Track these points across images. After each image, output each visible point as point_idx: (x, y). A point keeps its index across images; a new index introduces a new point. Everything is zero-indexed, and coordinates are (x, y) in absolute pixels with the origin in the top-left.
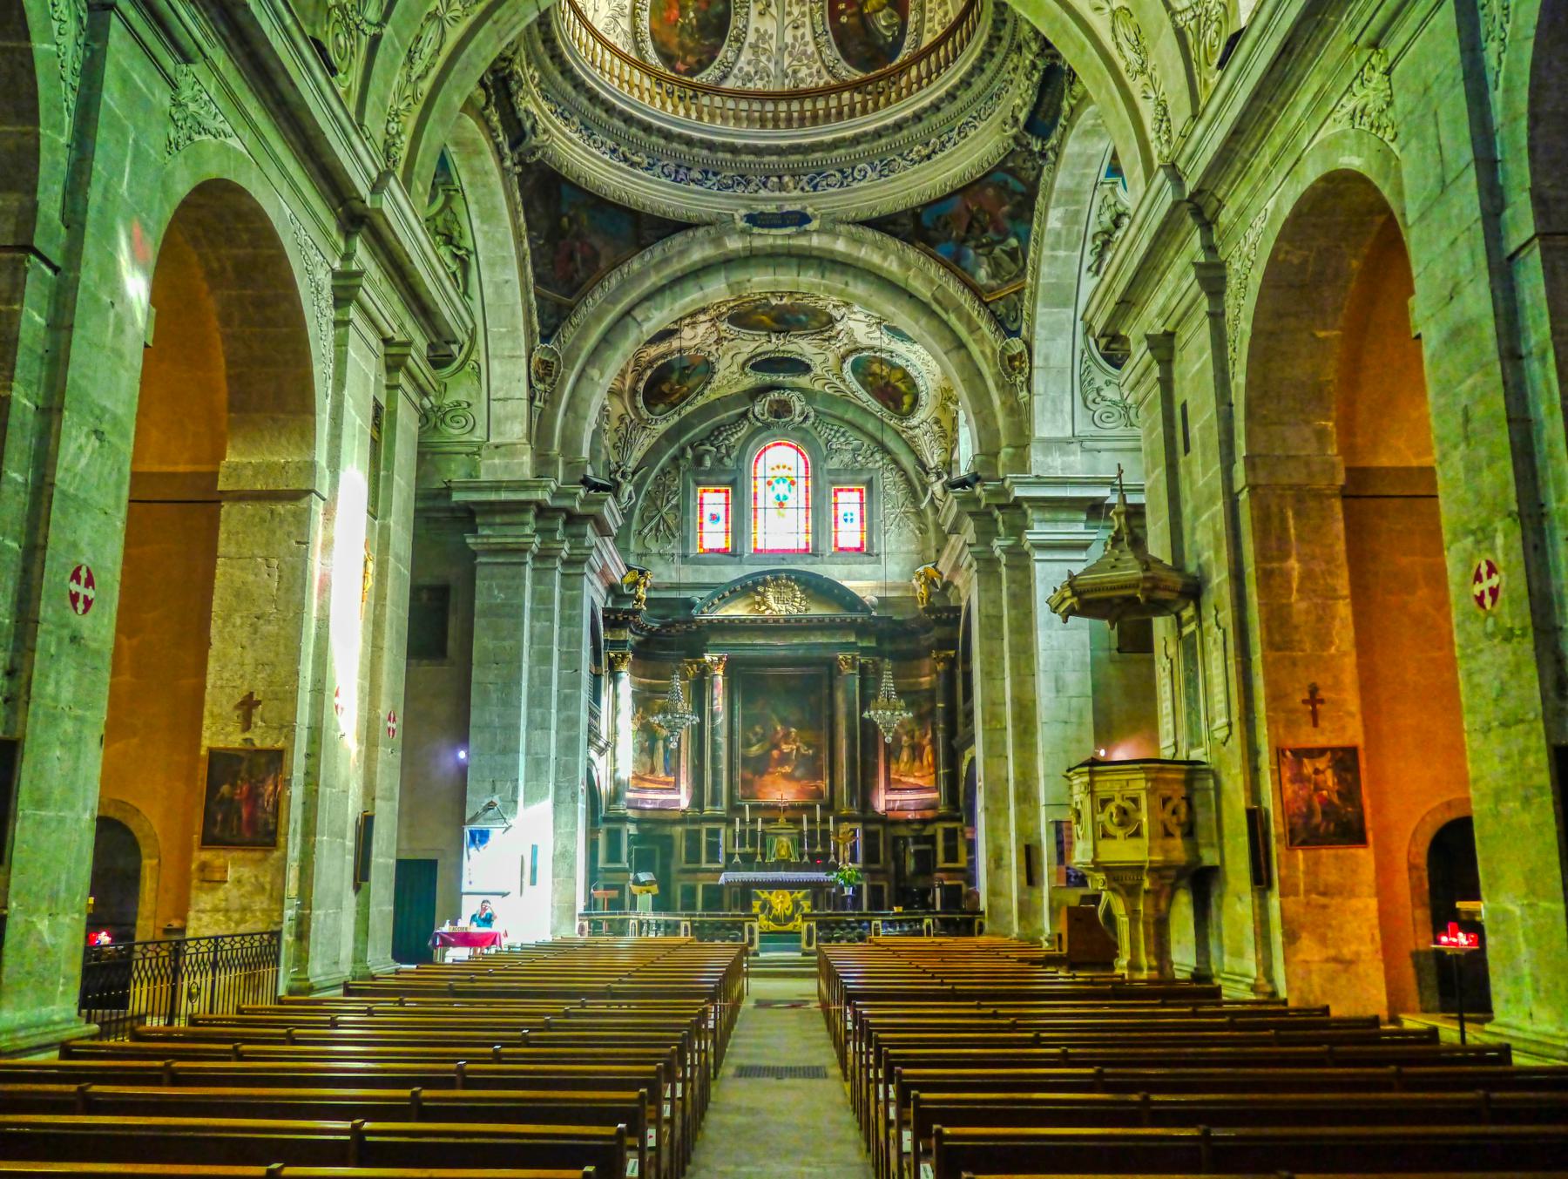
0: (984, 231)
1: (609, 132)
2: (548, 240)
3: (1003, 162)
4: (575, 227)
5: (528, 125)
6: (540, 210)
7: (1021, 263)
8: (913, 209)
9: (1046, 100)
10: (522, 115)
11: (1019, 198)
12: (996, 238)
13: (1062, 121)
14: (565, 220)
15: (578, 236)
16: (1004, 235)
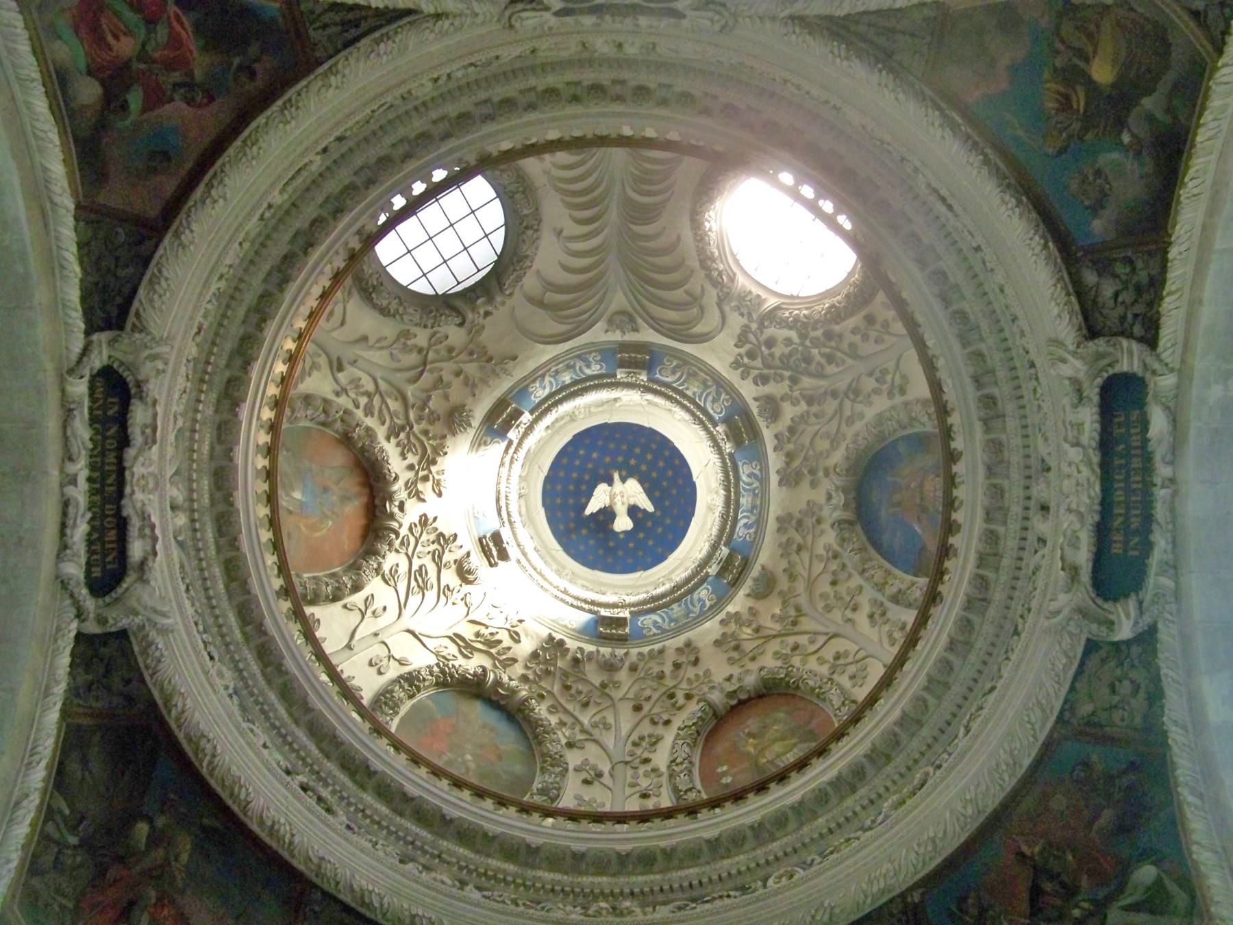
0: (1070, 892)
1: (285, 741)
2: (86, 844)
3: (1069, 705)
4: (159, 854)
5: (136, 549)
6: (96, 766)
7: (1180, 899)
8: (903, 895)
9: (1119, 496)
10: (128, 511)
11: (1125, 781)
12: (1101, 895)
13: (1163, 471)
14: (142, 829)
15: (158, 874)
16: (1125, 868)
